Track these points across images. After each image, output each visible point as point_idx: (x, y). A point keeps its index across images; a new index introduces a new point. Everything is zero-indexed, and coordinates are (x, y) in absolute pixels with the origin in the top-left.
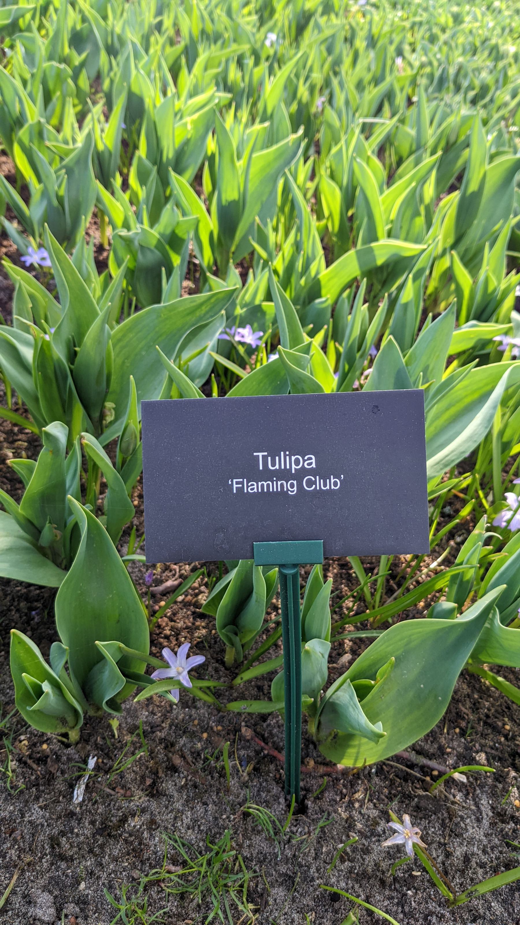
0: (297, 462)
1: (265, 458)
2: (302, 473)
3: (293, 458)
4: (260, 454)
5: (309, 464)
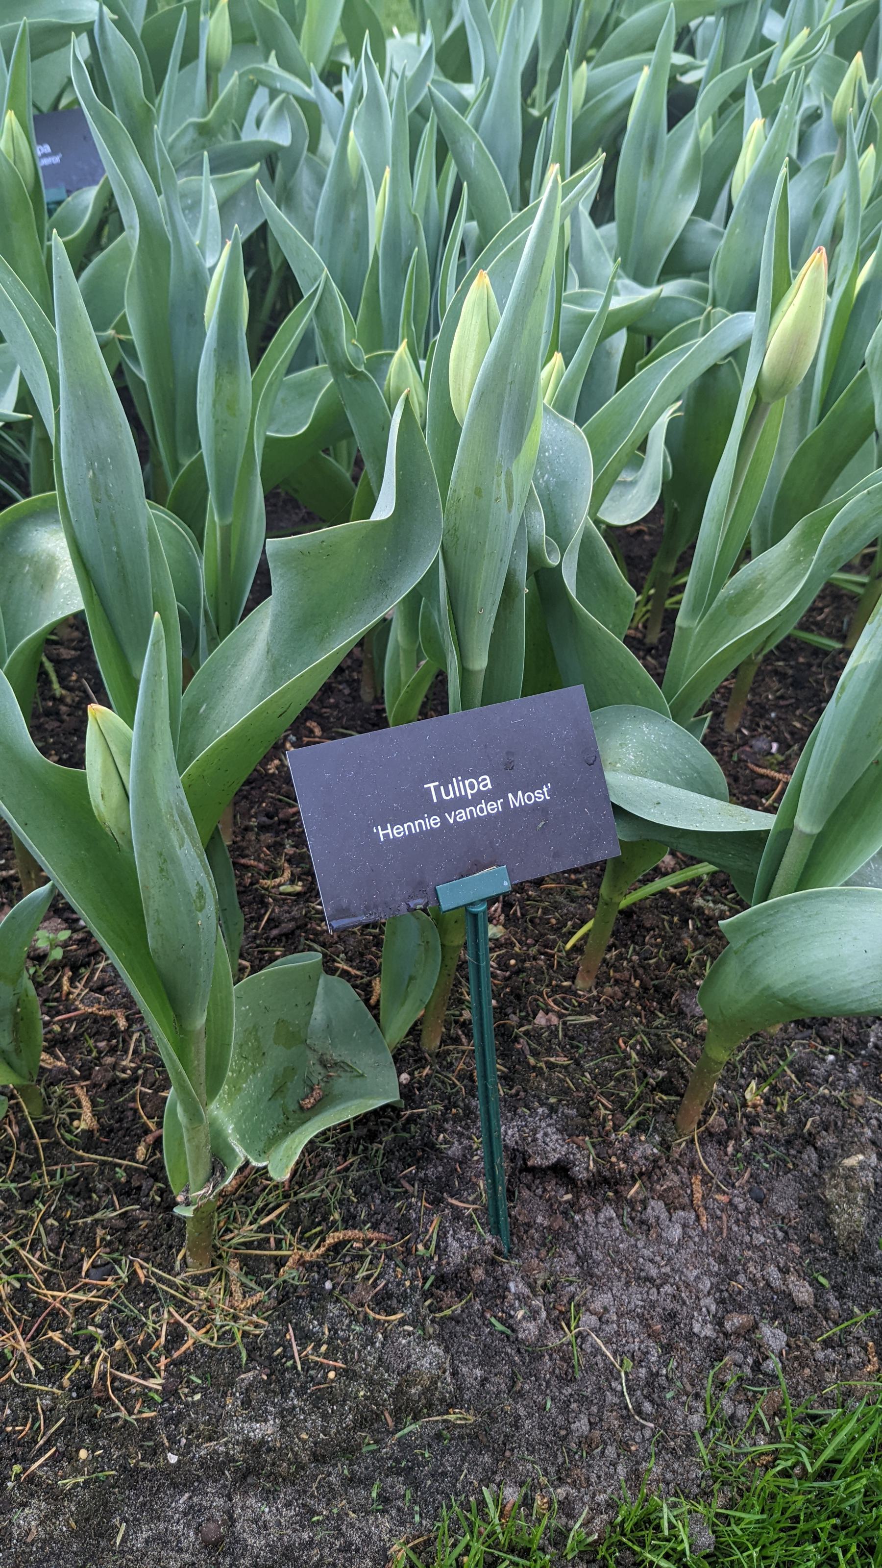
0: (472, 787)
1: (437, 789)
2: (480, 797)
3: (467, 782)
4: (431, 785)
5: (485, 786)
